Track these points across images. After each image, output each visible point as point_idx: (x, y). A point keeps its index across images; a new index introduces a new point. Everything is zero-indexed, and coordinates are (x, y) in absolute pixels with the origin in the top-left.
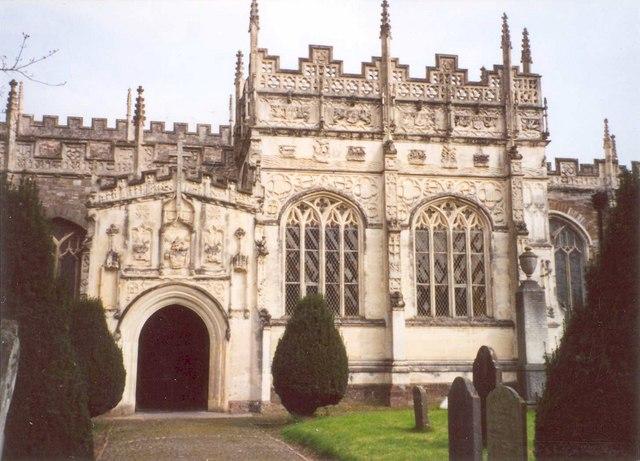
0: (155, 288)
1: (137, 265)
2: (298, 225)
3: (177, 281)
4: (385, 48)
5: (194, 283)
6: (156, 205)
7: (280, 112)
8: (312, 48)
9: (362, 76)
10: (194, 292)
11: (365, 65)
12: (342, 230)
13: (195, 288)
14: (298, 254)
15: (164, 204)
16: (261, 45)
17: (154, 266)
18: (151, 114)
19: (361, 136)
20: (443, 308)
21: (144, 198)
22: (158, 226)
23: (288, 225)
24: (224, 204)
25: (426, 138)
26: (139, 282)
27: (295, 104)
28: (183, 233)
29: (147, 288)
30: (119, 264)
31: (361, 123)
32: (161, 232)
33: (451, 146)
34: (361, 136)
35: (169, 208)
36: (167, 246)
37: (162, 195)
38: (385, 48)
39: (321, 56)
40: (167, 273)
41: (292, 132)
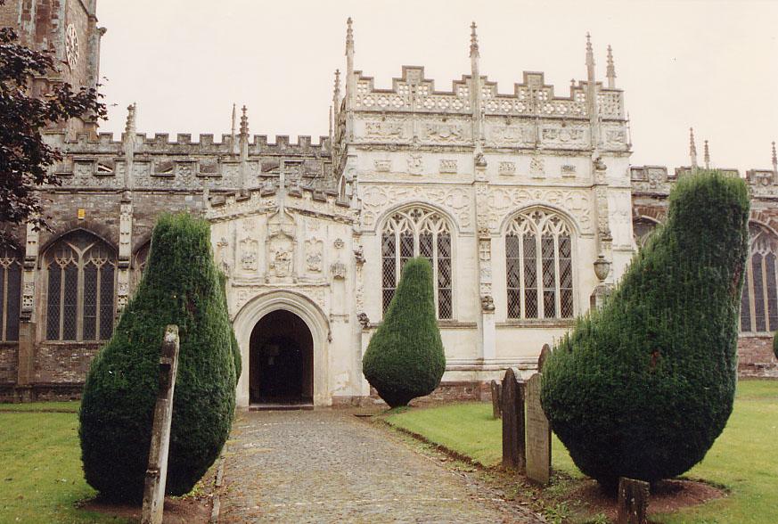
0: (263, 295)
2: (393, 235)
4: (474, 66)
6: (260, 220)
7: (375, 129)
8: (405, 69)
9: (453, 94)
10: (295, 297)
11: (456, 83)
12: (435, 239)
13: (298, 295)
14: (393, 261)
16: (355, 68)
18: (253, 130)
20: (532, 311)
25: (516, 151)
27: (389, 121)
29: (255, 295)
33: (539, 158)
35: (275, 221)
36: (273, 257)
38: (474, 66)
39: (413, 75)
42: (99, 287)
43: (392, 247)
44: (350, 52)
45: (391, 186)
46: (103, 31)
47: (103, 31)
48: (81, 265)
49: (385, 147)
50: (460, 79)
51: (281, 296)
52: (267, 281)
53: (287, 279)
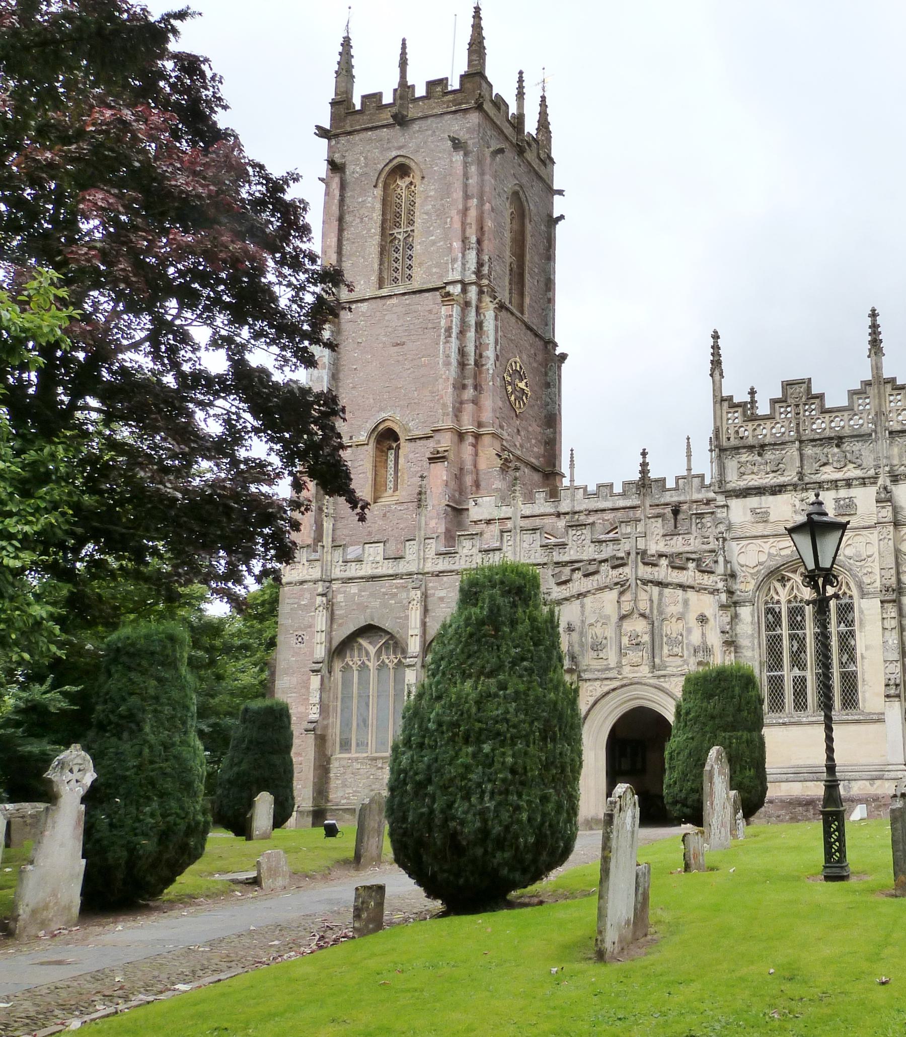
0: (614, 690)
1: (595, 665)
2: (778, 602)
3: (636, 680)
5: (652, 681)
8: (788, 385)
9: (849, 409)
11: (852, 393)
14: (779, 637)
15: (621, 593)
16: (725, 394)
17: (612, 662)
19: (848, 483)
20: (800, 703)
21: (597, 590)
22: (615, 618)
23: (766, 603)
24: (682, 587)
26: (598, 683)
28: (639, 626)
29: (606, 689)
30: (576, 665)
31: (851, 466)
32: (620, 627)
34: (848, 483)
35: (627, 597)
36: (625, 641)
37: (616, 584)
38: (877, 368)
40: (627, 671)
41: (760, 491)
42: (355, 686)
43: (777, 616)
44: (717, 377)
45: (772, 540)
46: (563, 357)
47: (563, 357)
48: (372, 665)
49: (760, 491)
50: (858, 386)
51: (635, 690)
52: (619, 673)
53: (641, 668)
